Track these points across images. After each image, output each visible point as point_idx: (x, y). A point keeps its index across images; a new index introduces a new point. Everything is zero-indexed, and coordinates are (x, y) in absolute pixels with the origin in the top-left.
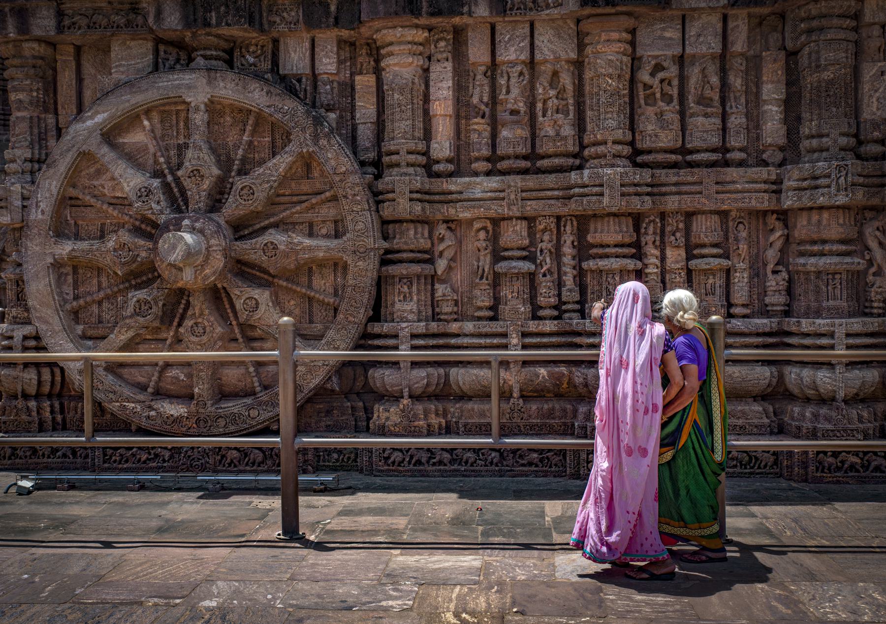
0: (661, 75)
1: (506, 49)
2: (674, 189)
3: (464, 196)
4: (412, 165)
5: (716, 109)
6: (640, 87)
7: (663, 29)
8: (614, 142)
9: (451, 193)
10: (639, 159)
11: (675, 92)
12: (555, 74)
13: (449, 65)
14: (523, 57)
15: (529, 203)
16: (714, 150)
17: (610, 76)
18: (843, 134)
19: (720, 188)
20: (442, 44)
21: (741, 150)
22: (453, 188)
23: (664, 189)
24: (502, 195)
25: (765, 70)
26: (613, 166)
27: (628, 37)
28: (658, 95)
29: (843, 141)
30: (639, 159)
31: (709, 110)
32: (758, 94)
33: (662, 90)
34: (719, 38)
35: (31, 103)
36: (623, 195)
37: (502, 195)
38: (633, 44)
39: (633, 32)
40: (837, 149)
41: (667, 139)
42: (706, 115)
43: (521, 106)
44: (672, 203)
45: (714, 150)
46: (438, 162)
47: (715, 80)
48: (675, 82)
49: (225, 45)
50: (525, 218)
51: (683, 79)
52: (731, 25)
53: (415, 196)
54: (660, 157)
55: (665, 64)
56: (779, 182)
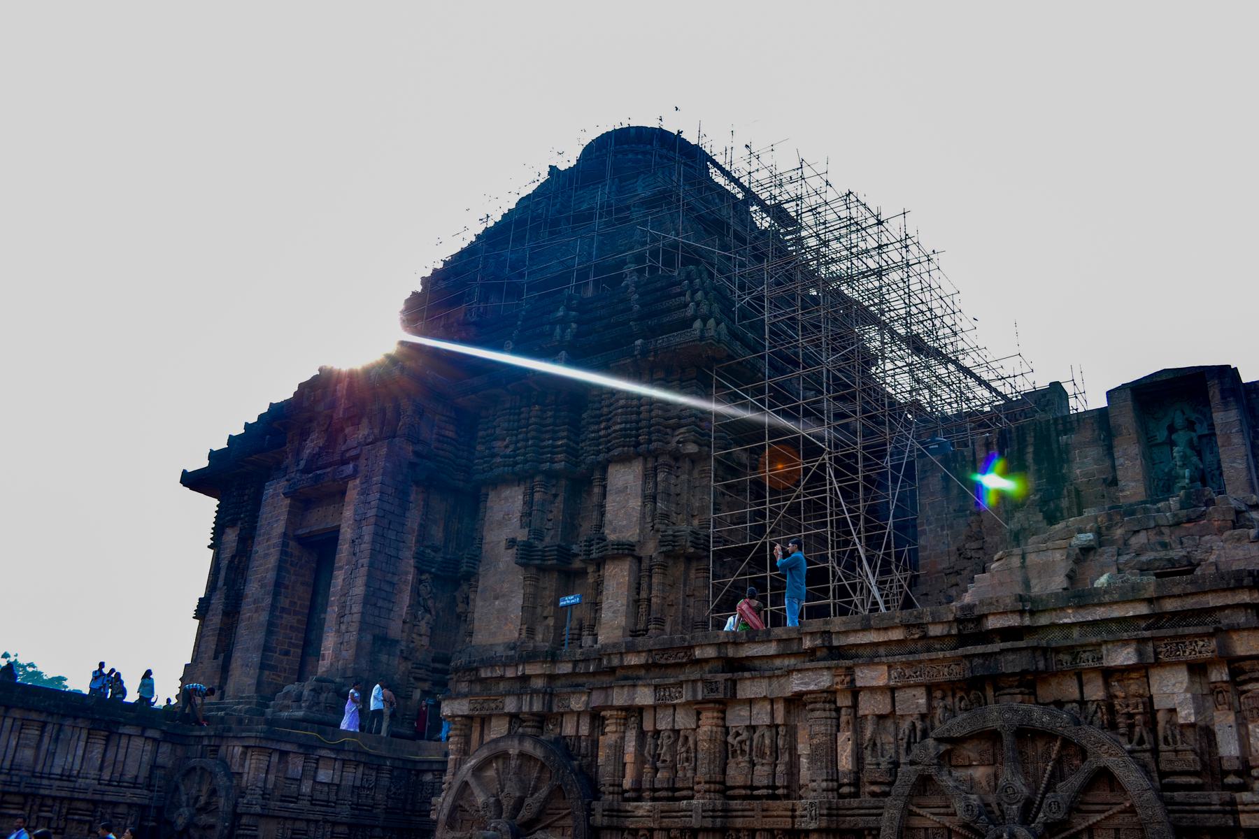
0: (738, 738)
1: (661, 723)
2: (739, 813)
3: (636, 814)
4: (613, 793)
5: (768, 759)
6: (730, 747)
7: (740, 710)
8: (706, 783)
9: (629, 812)
10: (730, 793)
11: (747, 749)
12: (686, 738)
13: (634, 732)
14: (669, 728)
15: (664, 820)
16: (767, 787)
17: (705, 741)
18: (823, 781)
19: (764, 813)
20: (633, 719)
21: (784, 787)
22: (629, 808)
23: (735, 814)
24: (651, 814)
25: (799, 736)
26: (703, 798)
27: (720, 715)
28: (739, 752)
29: (824, 785)
30: (730, 793)
31: (764, 761)
32: (796, 749)
33: (741, 747)
34: (769, 716)
35: (456, 751)
36: (704, 817)
37: (651, 814)
38: (724, 719)
39: (724, 712)
40: (821, 791)
41: (740, 781)
42: (763, 764)
43: (668, 758)
44: (739, 823)
45: (767, 787)
46: (627, 791)
47: (767, 742)
48: (748, 743)
49: (538, 719)
50: (661, 829)
51: (752, 740)
52: (775, 707)
53: (606, 813)
54: (737, 792)
55: (740, 732)
56: (794, 810)
